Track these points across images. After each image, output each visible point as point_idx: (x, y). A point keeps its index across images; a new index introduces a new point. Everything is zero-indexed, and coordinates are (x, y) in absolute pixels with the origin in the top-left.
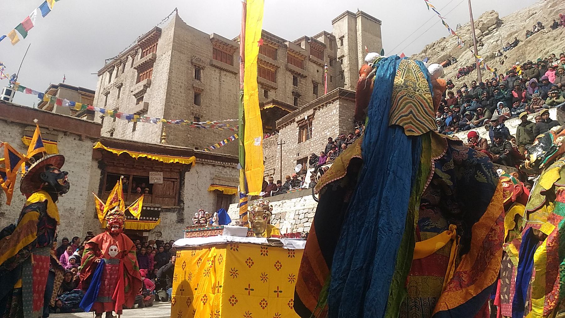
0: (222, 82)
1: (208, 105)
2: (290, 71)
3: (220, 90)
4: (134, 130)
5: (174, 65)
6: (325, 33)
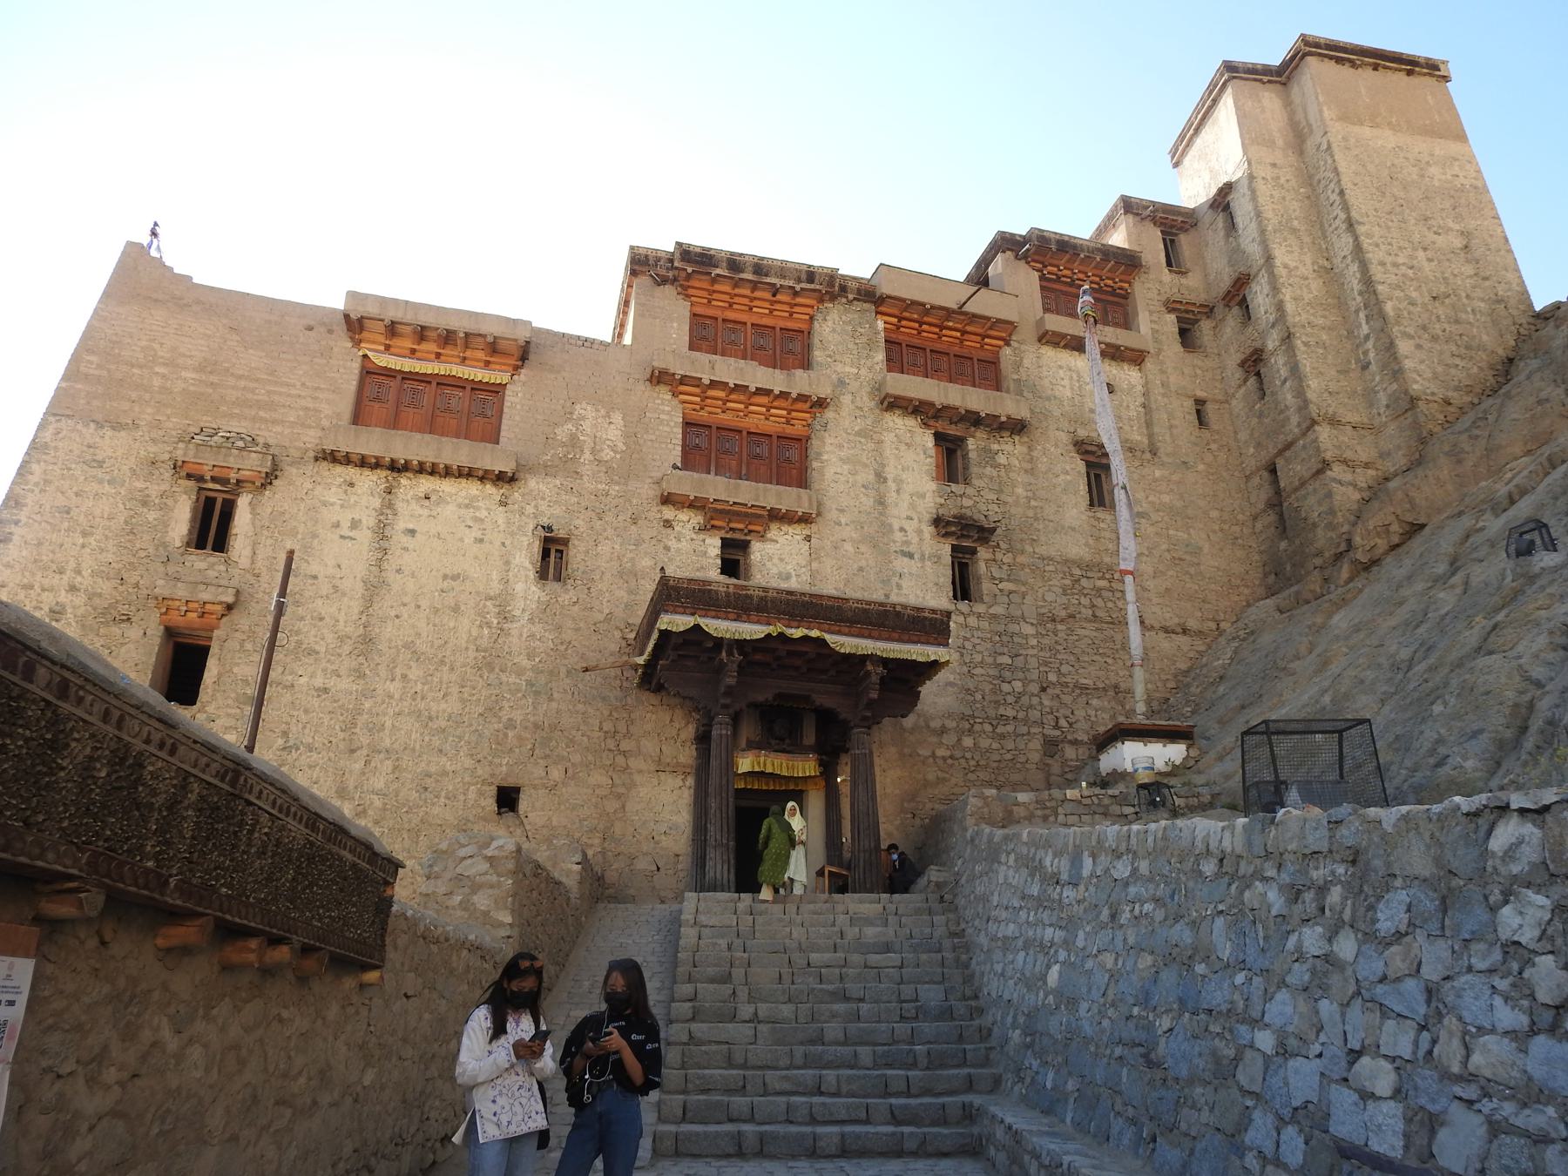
0: (398, 538)
5: (30, 500)
6: (1129, 206)
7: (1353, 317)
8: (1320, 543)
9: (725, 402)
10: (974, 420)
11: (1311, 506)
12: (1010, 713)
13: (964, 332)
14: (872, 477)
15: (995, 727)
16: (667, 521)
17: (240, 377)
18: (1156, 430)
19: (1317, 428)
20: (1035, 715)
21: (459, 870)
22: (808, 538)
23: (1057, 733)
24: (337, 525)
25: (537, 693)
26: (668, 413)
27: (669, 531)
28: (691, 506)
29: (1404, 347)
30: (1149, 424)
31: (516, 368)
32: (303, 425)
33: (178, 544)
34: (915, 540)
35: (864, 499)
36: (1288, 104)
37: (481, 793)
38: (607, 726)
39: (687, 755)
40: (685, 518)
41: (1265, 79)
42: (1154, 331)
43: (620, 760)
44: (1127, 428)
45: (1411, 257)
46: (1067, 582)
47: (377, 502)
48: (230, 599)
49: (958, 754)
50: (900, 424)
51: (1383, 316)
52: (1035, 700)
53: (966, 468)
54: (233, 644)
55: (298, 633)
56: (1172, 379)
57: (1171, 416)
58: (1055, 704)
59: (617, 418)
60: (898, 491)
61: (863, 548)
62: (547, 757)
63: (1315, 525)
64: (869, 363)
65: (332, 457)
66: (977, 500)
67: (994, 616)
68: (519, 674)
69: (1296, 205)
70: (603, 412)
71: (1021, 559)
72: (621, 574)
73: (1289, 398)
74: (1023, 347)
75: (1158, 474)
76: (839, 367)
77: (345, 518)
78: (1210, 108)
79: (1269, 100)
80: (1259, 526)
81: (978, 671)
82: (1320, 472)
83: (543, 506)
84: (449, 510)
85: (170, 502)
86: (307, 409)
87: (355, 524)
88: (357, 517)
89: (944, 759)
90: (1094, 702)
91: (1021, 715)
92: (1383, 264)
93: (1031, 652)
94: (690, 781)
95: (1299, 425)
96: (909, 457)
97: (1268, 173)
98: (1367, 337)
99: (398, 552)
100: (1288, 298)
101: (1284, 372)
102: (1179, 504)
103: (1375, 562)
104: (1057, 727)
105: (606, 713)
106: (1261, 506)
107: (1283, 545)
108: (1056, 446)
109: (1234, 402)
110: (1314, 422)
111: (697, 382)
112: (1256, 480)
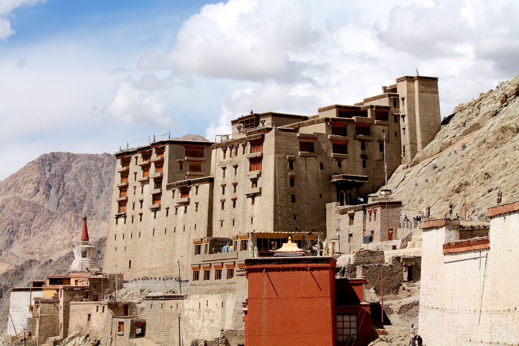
2: (358, 139)
4: (253, 203)
39: (335, 190)
50: (357, 142)
84: (311, 161)
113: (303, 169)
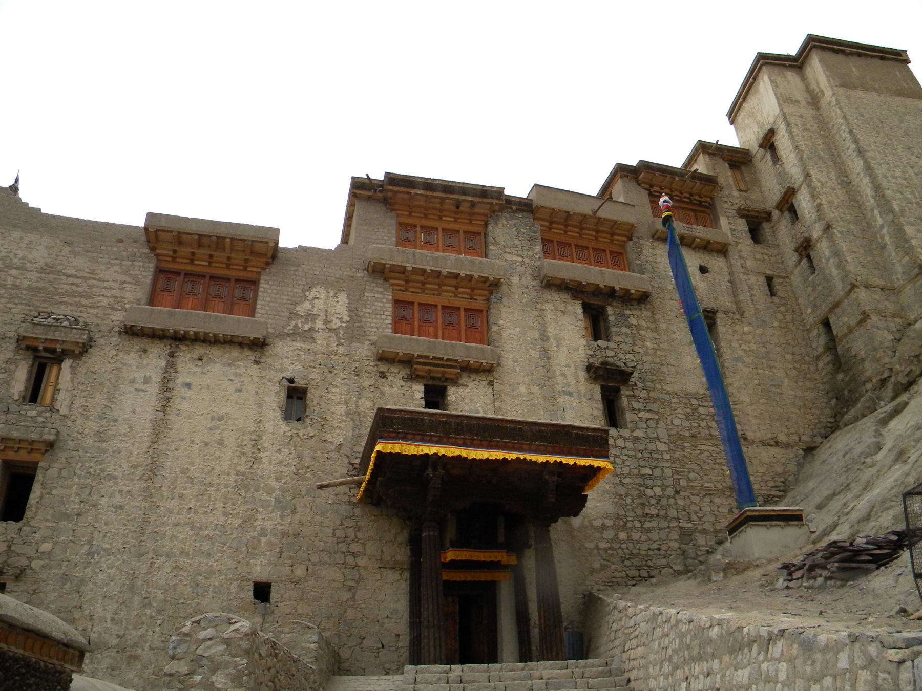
1: (74, 507)
3: (159, 428)
6: (703, 148)
7: (869, 214)
8: (868, 374)
9: (423, 283)
10: (611, 293)
11: (858, 345)
12: (653, 511)
13: (597, 232)
14: (537, 335)
15: (642, 523)
16: (383, 373)
17: (69, 276)
18: (741, 298)
19: (856, 289)
20: (672, 513)
21: (199, 652)
22: (491, 383)
23: (690, 525)
24: (133, 381)
25: (283, 509)
26: (381, 293)
27: (384, 380)
28: (401, 362)
29: (909, 230)
30: (735, 295)
31: (267, 264)
32: (112, 308)
33: (16, 397)
34: (574, 382)
35: (532, 352)
36: (804, 79)
37: (241, 588)
38: (340, 533)
39: (402, 554)
40: (396, 370)
41: (787, 63)
42: (732, 230)
43: (350, 560)
44: (721, 298)
45: (904, 172)
46: (689, 410)
47: (163, 363)
48: (52, 438)
49: (616, 546)
51: (892, 211)
52: (672, 501)
53: (607, 329)
54: (53, 472)
55: (102, 462)
56: (749, 263)
57: (751, 288)
58: (688, 502)
59: (343, 298)
60: (558, 346)
61: (535, 389)
62: (291, 558)
63: (863, 360)
64: (530, 254)
65: (131, 332)
66: (617, 350)
67: (637, 438)
68: (269, 494)
69: (820, 142)
70: (332, 293)
71: (652, 394)
72: (348, 414)
73: (835, 272)
74: (642, 241)
75: (746, 329)
76: (508, 257)
77: (139, 376)
78: (752, 84)
79: (791, 76)
80: (821, 365)
81: (627, 481)
82: (861, 322)
83: (286, 363)
84: (217, 368)
85: (13, 367)
86: (117, 297)
87: (147, 380)
88: (148, 374)
89: (606, 550)
90: (716, 500)
91: (662, 513)
92: (886, 177)
93: (666, 464)
94: (407, 575)
95: (843, 289)
96: (566, 320)
97: (799, 122)
98: (882, 227)
99: (178, 401)
100: (824, 202)
101: (827, 253)
102: (763, 350)
103: (910, 384)
104: (690, 520)
105: (338, 522)
106: (821, 349)
107: (840, 376)
108: (671, 310)
109: (793, 278)
110: (853, 286)
111: (403, 270)
112: (815, 333)
113: (136, 404)
